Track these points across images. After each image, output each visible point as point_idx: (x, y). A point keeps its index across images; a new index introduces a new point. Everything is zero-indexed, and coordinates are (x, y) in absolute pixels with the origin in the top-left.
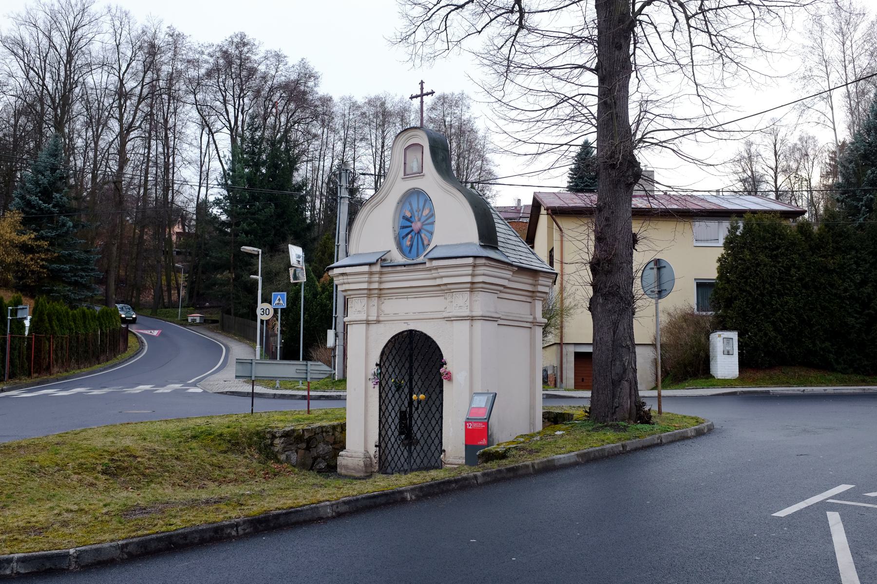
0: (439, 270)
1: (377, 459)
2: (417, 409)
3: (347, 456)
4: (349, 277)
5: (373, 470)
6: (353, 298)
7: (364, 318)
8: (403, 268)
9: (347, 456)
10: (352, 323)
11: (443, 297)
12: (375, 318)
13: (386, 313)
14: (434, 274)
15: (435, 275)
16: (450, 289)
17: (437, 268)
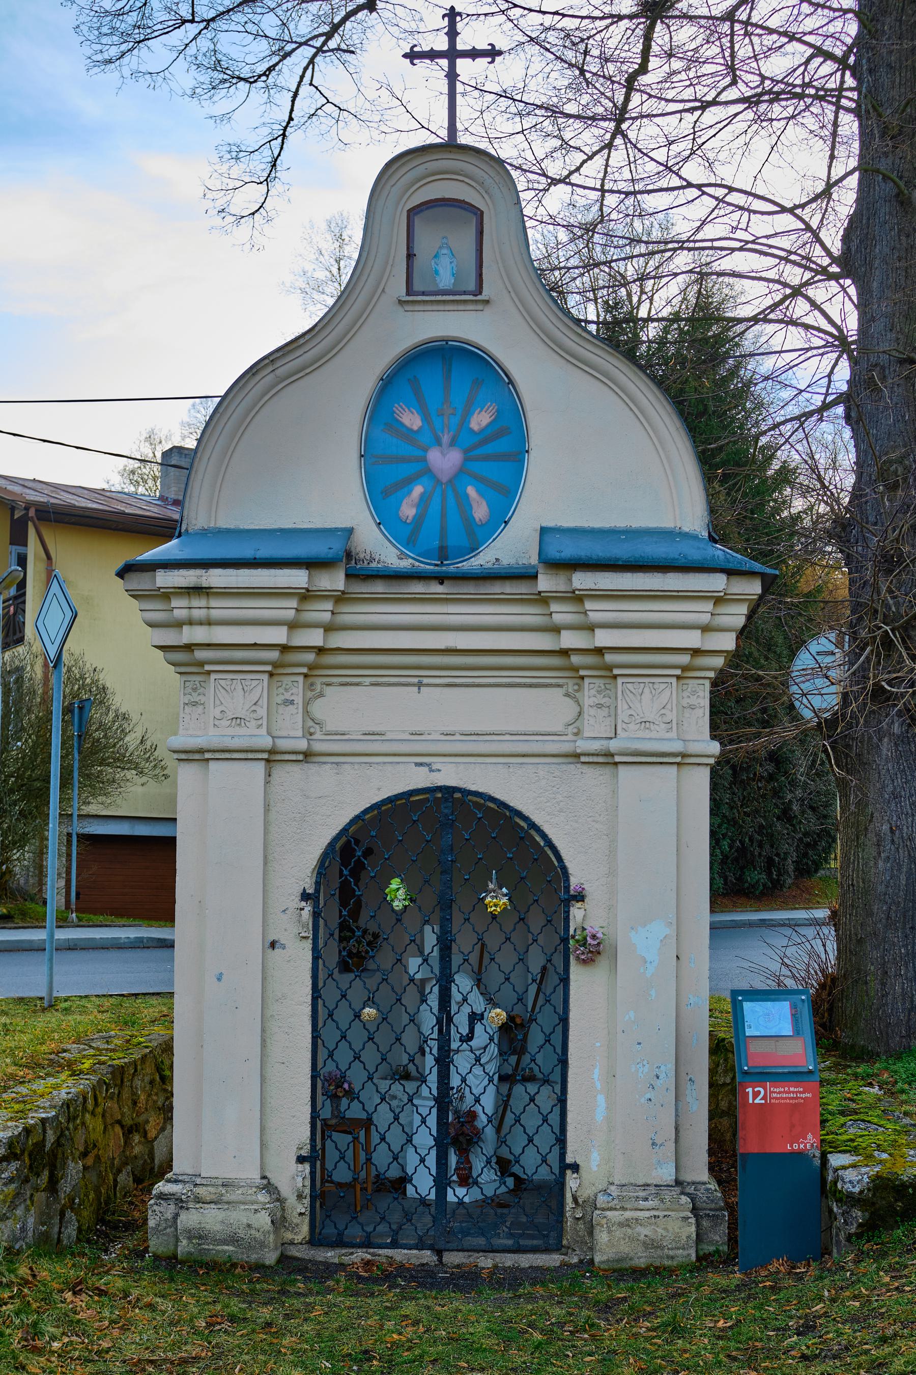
0: (589, 605)
1: (307, 1201)
2: (469, 1037)
4: (214, 603)
5: (289, 1236)
7: (267, 742)
8: (436, 588)
10: (207, 756)
11: (559, 692)
12: (303, 745)
13: (330, 727)
14: (562, 613)
17: (577, 598)
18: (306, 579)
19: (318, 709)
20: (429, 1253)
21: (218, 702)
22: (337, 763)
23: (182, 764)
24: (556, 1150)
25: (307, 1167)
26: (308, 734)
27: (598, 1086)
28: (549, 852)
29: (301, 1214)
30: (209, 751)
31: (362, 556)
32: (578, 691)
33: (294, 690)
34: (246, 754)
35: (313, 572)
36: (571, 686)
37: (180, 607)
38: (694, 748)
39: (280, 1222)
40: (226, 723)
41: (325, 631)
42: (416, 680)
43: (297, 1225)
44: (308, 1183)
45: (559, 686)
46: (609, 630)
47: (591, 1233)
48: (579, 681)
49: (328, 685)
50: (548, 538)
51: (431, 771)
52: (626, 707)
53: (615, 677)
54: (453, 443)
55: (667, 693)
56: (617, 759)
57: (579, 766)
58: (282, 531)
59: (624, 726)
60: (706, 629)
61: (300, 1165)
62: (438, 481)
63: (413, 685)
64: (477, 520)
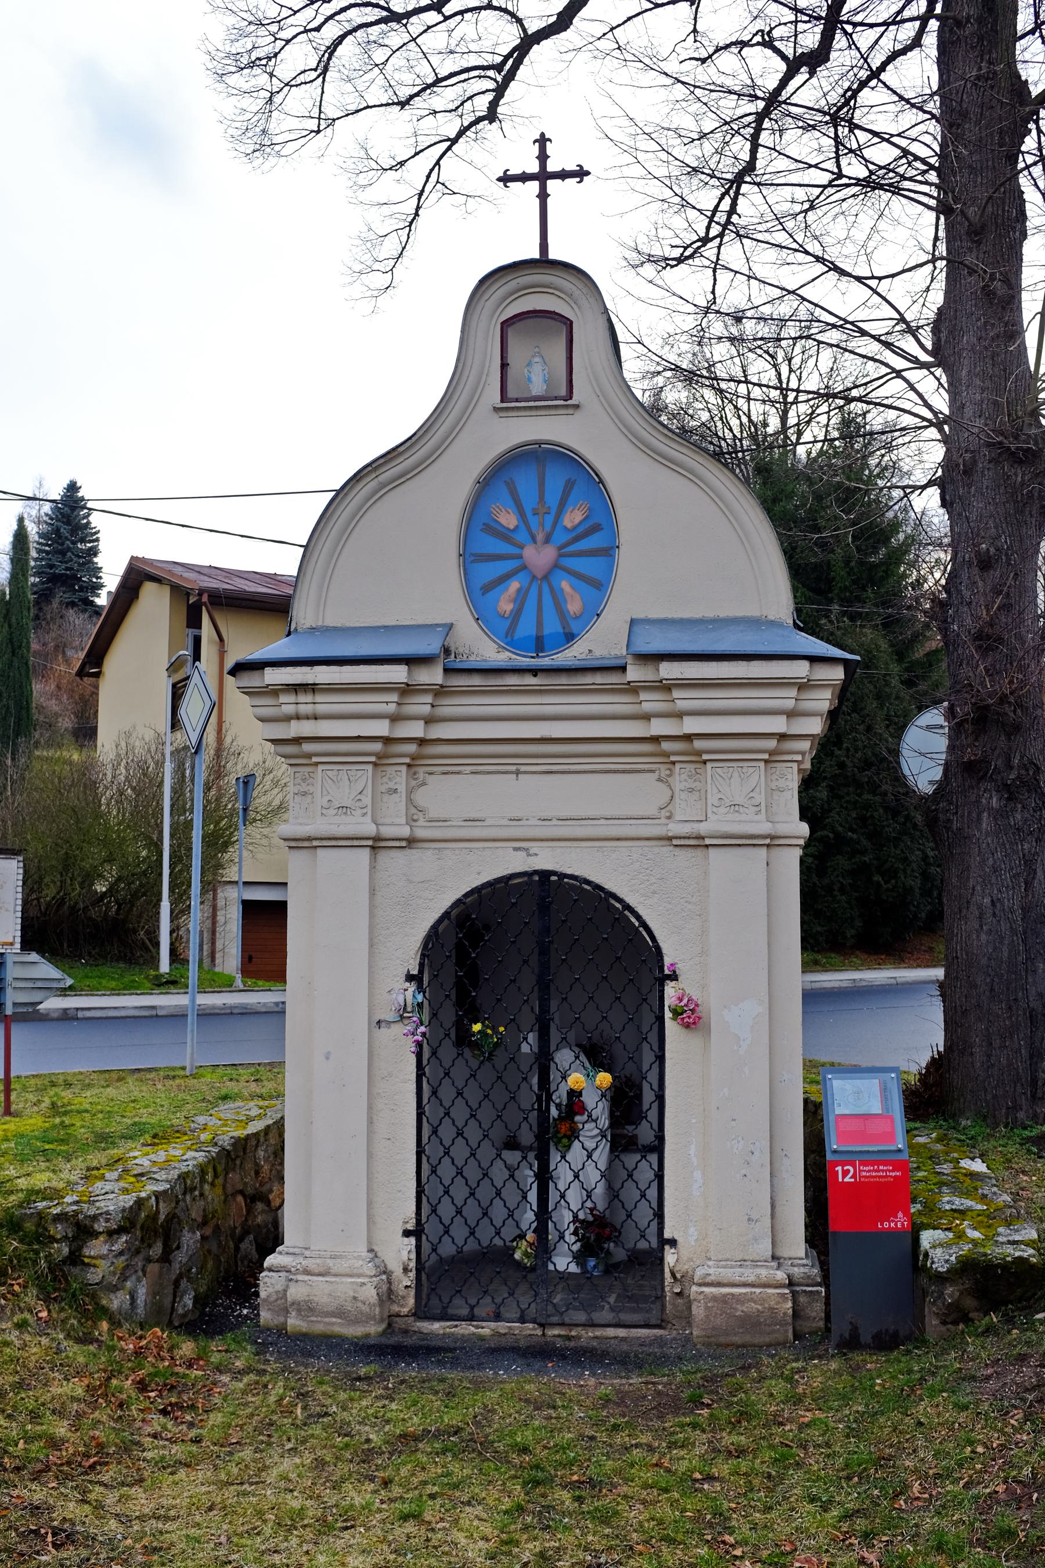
0: (676, 694)
1: (412, 1275)
3: (307, 1272)
4: (319, 698)
5: (395, 1308)
6: (317, 764)
7: (370, 829)
8: (530, 680)
9: (307, 1272)
10: (315, 843)
12: (405, 832)
13: (433, 814)
14: (651, 702)
15: (647, 707)
16: (309, 756)
17: (666, 687)
18: (405, 674)
19: (421, 797)
20: (531, 1326)
21: (325, 793)
22: (439, 849)
23: (292, 851)
24: (654, 1225)
25: (412, 1240)
26: (411, 821)
27: (695, 1160)
28: (644, 933)
29: (407, 1287)
30: (316, 839)
31: (461, 650)
32: (670, 776)
33: (398, 779)
34: (351, 842)
35: (413, 668)
36: (664, 772)
37: (288, 704)
38: (782, 829)
39: (388, 1295)
40: (332, 812)
41: (426, 723)
42: (514, 768)
43: (403, 1297)
44: (413, 1256)
45: (653, 771)
46: (697, 717)
47: (689, 1308)
48: (670, 766)
49: (430, 774)
50: (636, 629)
51: (529, 855)
52: (715, 791)
53: (705, 762)
54: (547, 540)
55: (756, 777)
56: (708, 842)
57: (671, 848)
58: (385, 627)
59: (715, 809)
60: (791, 714)
61: (406, 1239)
62: (534, 577)
63: (511, 772)
64: (572, 613)
